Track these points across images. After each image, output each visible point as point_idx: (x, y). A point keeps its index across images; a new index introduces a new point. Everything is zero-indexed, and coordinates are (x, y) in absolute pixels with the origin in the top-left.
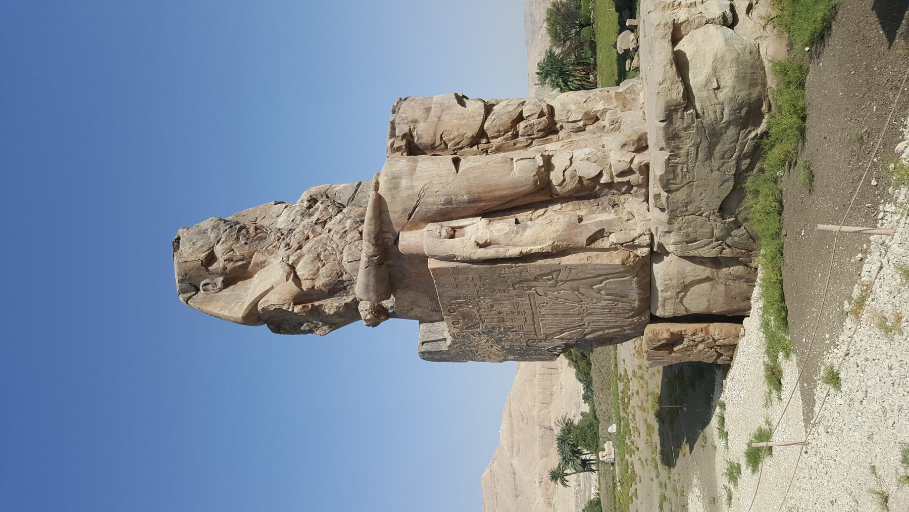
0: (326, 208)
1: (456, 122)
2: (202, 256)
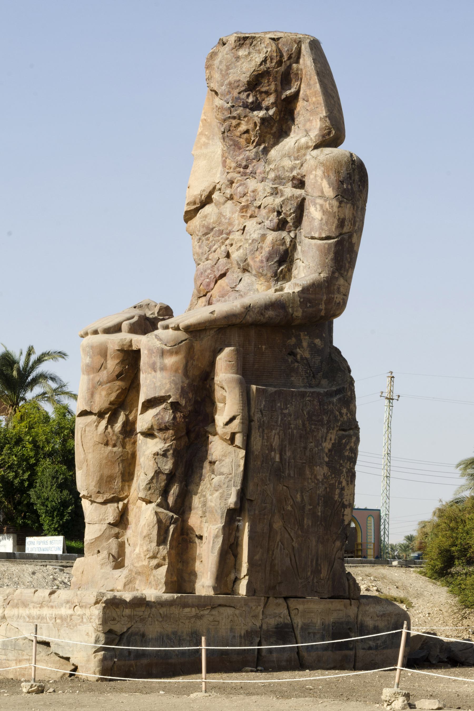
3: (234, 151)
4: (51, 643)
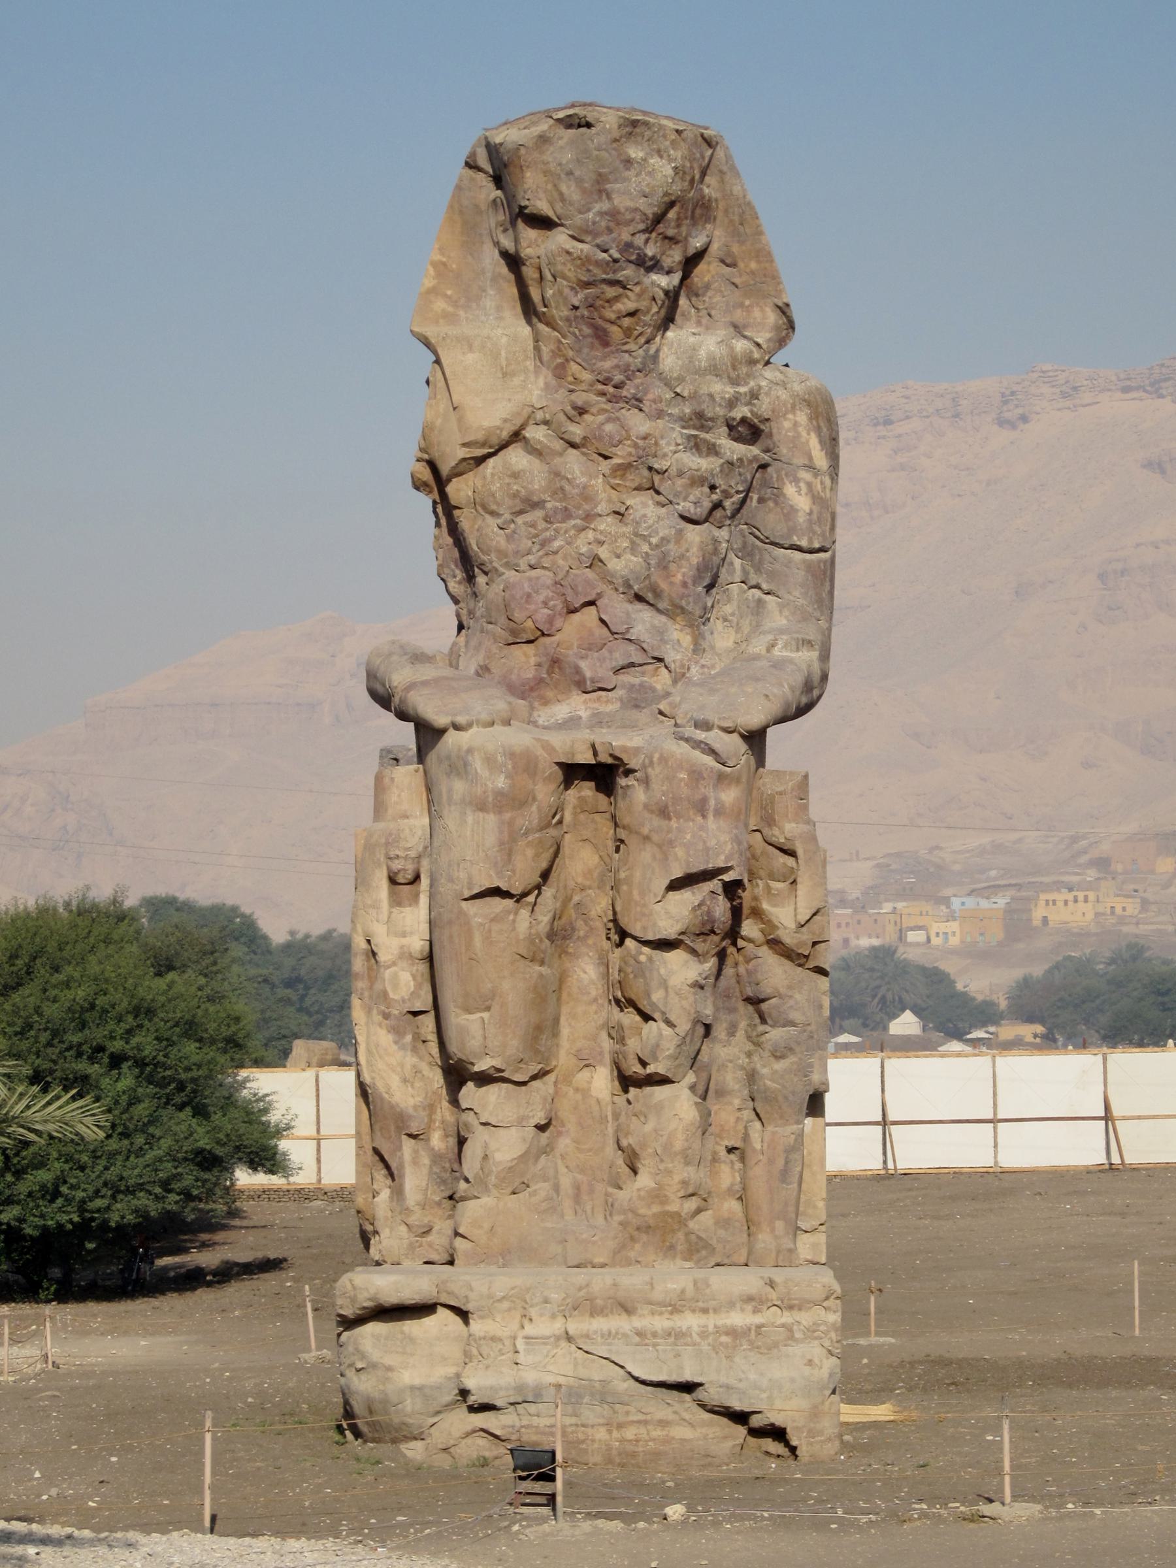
0: (698, 480)
1: (638, 874)
2: (542, 206)
3: (592, 347)
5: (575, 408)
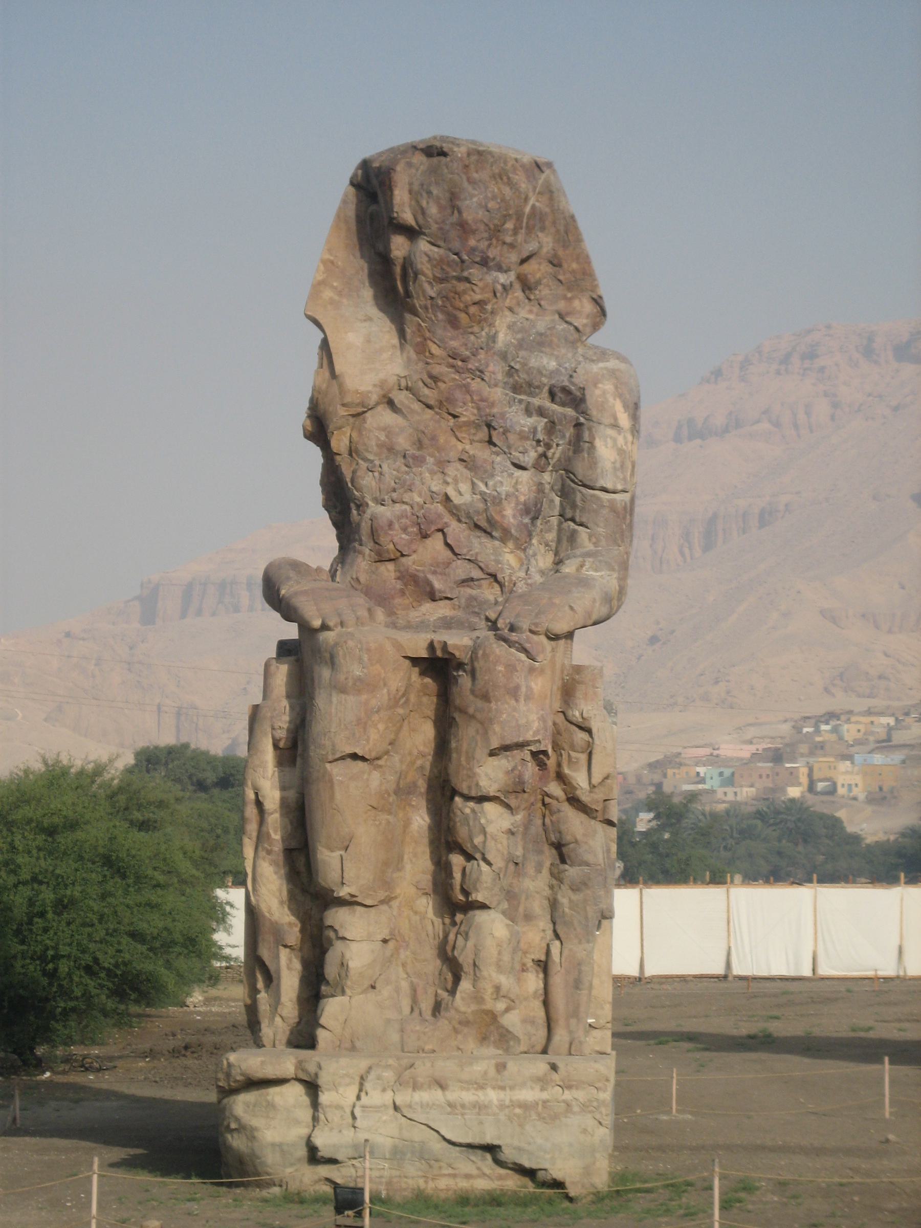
1: (465, 747)
2: (407, 217)
4: (503, 1148)
5: (431, 377)
